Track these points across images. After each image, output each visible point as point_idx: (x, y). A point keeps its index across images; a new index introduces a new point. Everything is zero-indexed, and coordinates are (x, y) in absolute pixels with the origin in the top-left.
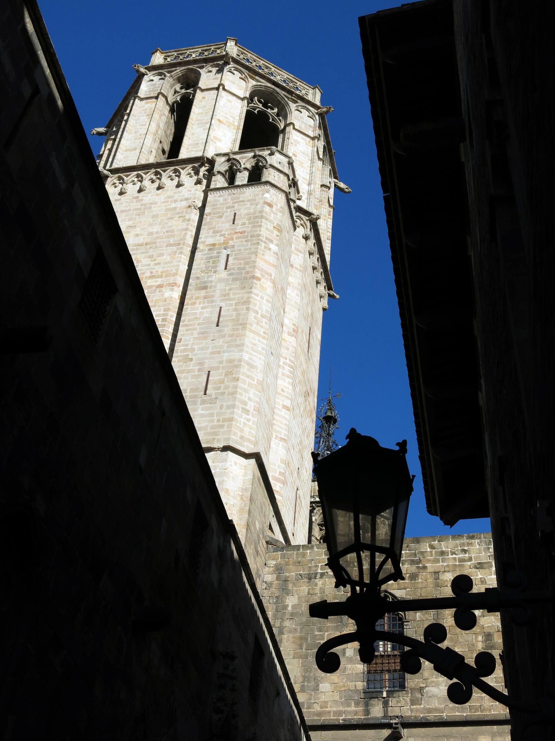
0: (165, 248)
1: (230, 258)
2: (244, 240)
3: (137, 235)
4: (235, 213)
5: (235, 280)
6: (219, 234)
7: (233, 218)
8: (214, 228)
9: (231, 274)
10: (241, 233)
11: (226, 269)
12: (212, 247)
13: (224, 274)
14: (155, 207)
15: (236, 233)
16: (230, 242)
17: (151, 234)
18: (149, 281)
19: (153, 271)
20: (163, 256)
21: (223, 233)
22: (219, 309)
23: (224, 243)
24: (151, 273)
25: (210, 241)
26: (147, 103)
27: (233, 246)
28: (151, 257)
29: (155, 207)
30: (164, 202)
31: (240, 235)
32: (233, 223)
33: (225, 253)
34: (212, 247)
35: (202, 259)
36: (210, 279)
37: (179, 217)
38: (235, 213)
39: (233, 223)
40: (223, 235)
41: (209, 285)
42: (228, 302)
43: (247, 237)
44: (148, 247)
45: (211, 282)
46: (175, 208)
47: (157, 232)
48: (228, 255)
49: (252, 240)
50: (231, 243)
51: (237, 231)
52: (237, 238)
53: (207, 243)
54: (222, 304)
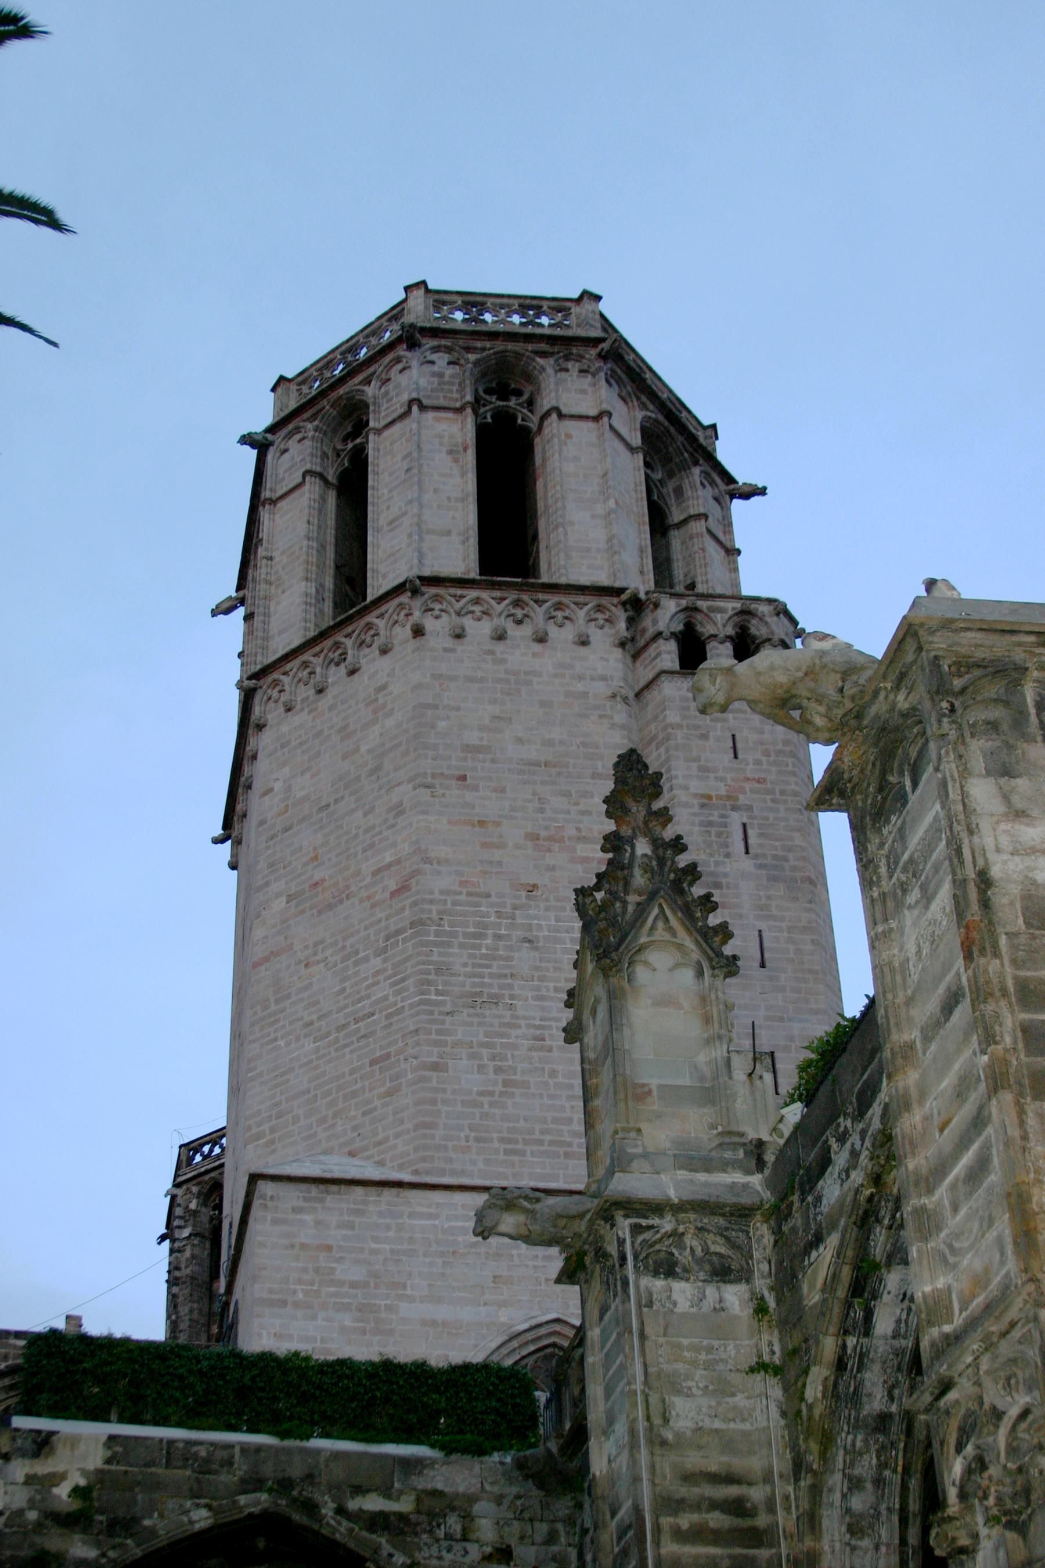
0: (589, 780)
1: (751, 832)
2: (768, 797)
3: (520, 741)
4: (733, 736)
5: (773, 879)
6: (712, 775)
7: (731, 745)
8: (698, 759)
9: (760, 866)
10: (758, 781)
11: (747, 852)
12: (705, 801)
13: (747, 864)
14: (538, 683)
15: (748, 779)
16: (741, 797)
17: (549, 743)
18: (579, 847)
19: (581, 826)
20: (592, 797)
21: (720, 774)
22: (757, 933)
23: (729, 798)
24: (578, 829)
25: (697, 786)
26: (438, 420)
27: (749, 808)
28: (567, 794)
29: (538, 683)
30: (556, 675)
31: (757, 785)
32: (736, 757)
33: (736, 819)
34: (705, 801)
35: (693, 824)
36: (721, 869)
37: (601, 717)
38: (733, 736)
39: (736, 757)
40: (722, 779)
41: (724, 881)
42: (772, 923)
43: (770, 792)
44: (553, 771)
45: (726, 875)
46: (585, 695)
47: (562, 742)
48: (744, 825)
49: (786, 801)
50: (742, 800)
51: (749, 776)
52: (753, 791)
53: (693, 790)
54: (763, 925)
